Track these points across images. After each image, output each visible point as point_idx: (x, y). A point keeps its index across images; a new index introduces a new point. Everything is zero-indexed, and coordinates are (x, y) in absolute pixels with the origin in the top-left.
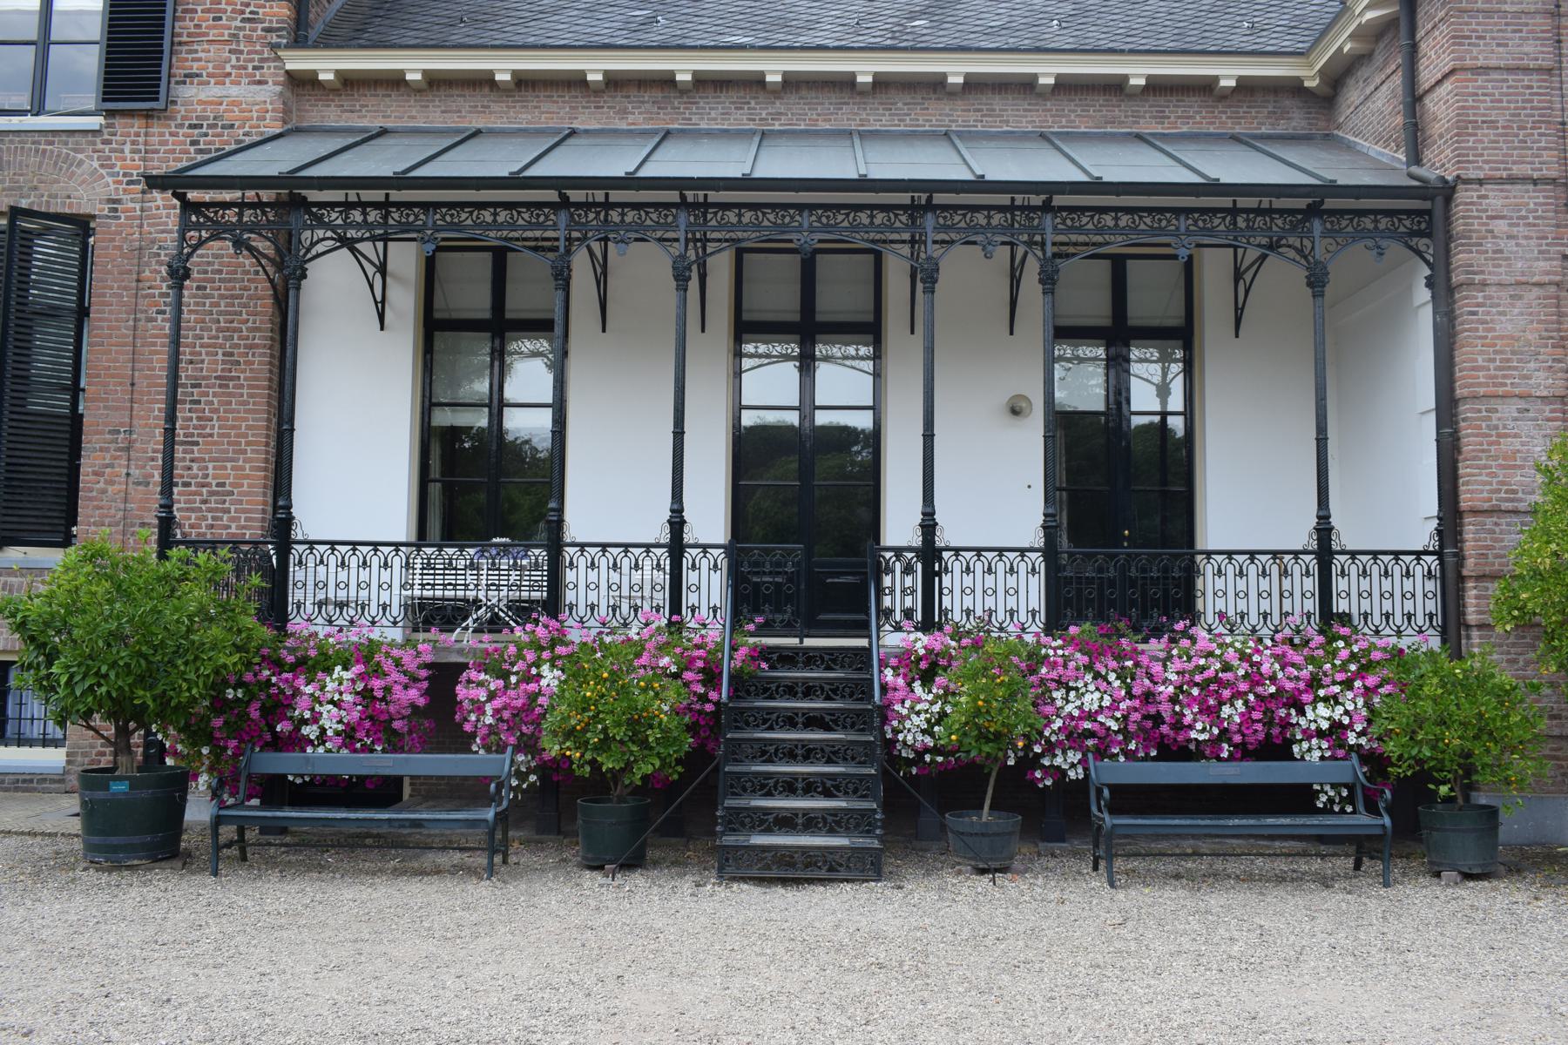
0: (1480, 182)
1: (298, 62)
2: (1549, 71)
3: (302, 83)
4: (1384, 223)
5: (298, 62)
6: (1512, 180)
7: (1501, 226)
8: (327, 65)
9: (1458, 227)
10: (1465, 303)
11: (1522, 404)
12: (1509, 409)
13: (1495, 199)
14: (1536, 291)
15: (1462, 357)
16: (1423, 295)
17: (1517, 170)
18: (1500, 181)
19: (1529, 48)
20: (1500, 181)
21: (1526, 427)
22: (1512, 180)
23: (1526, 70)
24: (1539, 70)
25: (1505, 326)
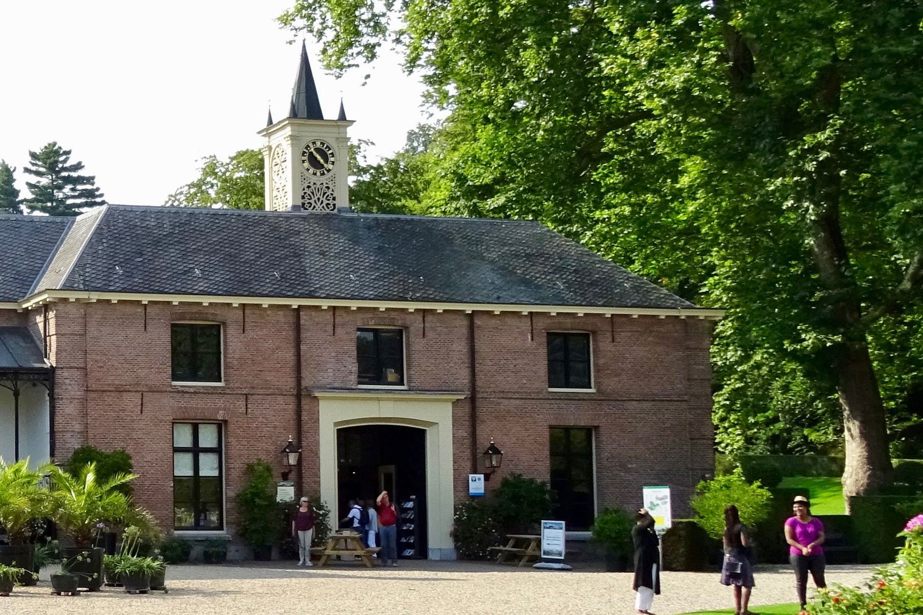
0: (62, 368)
2: (82, 335)
4: (36, 376)
6: (71, 368)
7: (67, 381)
9: (57, 381)
10: (59, 404)
13: (66, 374)
15: (57, 418)
16: (48, 398)
17: (72, 365)
18: (67, 368)
19: (77, 328)
20: (67, 368)
21: (73, 440)
22: (71, 368)
23: (76, 335)
24: (79, 335)
25: (68, 411)
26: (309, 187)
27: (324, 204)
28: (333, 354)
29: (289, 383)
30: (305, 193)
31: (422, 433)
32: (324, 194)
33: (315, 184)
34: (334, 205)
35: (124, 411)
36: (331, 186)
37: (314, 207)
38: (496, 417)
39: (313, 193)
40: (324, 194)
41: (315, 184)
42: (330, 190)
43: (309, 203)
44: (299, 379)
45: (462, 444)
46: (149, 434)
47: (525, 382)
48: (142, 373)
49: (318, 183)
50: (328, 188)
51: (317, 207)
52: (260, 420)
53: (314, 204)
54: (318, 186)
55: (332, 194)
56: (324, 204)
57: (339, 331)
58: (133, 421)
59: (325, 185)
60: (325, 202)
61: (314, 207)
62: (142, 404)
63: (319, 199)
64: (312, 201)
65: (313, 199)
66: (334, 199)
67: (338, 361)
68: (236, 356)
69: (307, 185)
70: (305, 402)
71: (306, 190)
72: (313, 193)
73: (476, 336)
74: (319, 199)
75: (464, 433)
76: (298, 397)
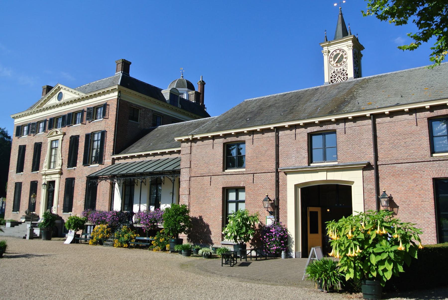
1: (113, 157)
3: (113, 159)
5: (113, 157)
7: (184, 173)
8: (115, 157)
11: (185, 195)
12: (184, 196)
14: (187, 181)
21: (185, 198)
26: (334, 72)
27: (342, 78)
28: (295, 149)
29: (273, 167)
30: (332, 75)
31: (350, 188)
32: (342, 73)
33: (337, 70)
34: (347, 78)
35: (204, 184)
36: (345, 69)
37: (337, 81)
38: (393, 175)
39: (336, 74)
40: (342, 73)
41: (337, 70)
42: (345, 71)
43: (344, 79)
44: (277, 164)
45: (371, 193)
46: (213, 194)
47: (412, 152)
48: (211, 167)
49: (339, 69)
50: (344, 70)
51: (338, 80)
52: (259, 185)
53: (337, 79)
54: (339, 70)
55: (346, 73)
56: (342, 78)
57: (298, 137)
58: (207, 189)
59: (342, 69)
60: (342, 77)
61: (337, 81)
62: (211, 181)
63: (339, 77)
64: (336, 78)
65: (336, 77)
66: (347, 75)
67: (298, 152)
68: (250, 156)
69: (333, 71)
70: (281, 175)
71: (333, 74)
72: (336, 74)
73: (377, 129)
74: (339, 77)
75: (372, 186)
76: (277, 173)
